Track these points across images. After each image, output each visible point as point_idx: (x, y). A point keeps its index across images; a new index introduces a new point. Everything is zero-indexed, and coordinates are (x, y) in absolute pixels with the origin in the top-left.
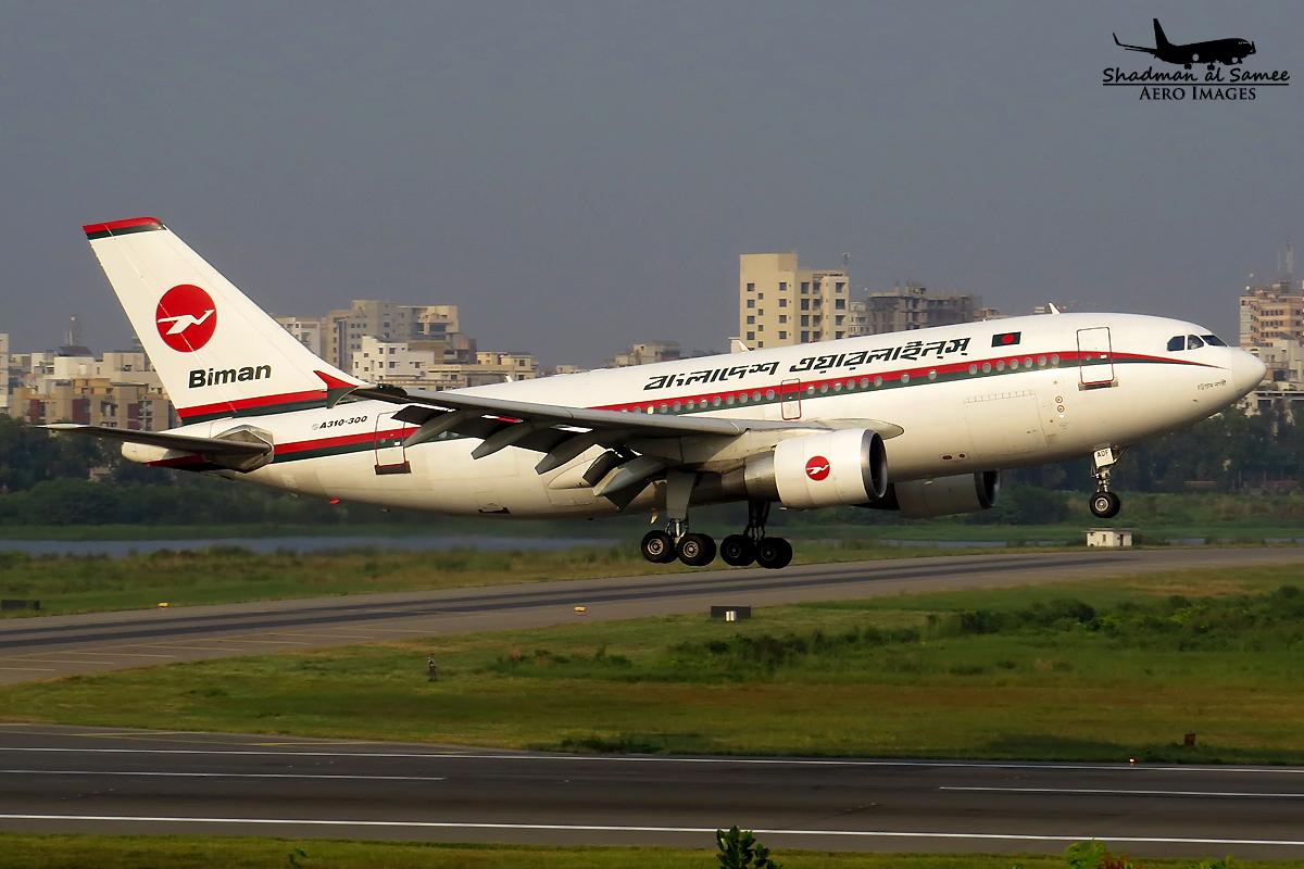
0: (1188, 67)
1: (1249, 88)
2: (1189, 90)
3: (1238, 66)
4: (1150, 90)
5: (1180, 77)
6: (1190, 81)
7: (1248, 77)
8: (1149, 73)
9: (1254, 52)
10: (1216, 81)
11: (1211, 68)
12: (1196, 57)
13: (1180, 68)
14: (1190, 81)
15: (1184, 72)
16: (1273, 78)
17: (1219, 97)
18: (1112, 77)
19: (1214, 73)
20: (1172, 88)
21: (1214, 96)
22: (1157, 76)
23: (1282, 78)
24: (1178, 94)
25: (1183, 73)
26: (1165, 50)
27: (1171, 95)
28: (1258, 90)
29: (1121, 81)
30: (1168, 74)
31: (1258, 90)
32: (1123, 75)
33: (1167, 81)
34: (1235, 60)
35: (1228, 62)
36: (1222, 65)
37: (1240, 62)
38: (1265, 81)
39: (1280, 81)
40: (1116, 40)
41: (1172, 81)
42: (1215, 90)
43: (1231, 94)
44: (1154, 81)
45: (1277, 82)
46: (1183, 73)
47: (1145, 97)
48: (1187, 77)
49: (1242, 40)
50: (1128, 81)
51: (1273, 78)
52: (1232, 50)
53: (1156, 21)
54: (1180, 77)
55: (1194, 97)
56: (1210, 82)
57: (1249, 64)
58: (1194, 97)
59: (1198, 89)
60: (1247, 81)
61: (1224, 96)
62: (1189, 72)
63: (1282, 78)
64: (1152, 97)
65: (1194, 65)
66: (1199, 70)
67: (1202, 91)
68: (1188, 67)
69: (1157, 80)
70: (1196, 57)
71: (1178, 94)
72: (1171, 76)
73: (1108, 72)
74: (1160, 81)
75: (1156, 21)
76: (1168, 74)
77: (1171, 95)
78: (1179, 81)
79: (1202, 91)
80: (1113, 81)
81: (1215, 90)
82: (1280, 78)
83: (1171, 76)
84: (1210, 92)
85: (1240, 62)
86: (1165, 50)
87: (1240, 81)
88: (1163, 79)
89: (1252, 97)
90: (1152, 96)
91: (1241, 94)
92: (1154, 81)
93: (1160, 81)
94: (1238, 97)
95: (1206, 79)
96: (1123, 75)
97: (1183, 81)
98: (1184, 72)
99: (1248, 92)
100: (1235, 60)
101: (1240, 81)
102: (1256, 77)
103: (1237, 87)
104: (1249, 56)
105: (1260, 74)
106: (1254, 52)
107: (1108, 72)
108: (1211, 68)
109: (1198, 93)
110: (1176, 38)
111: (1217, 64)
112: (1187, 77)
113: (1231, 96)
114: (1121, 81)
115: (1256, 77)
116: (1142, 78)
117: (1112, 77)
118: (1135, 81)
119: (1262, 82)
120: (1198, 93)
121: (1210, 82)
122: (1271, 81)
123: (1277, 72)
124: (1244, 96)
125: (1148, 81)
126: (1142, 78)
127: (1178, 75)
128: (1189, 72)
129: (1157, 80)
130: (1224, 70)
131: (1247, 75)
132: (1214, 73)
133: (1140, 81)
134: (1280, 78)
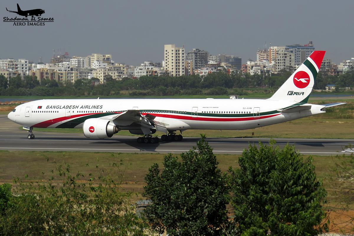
0: (26, 17)
1: (43, 22)
2: (27, 23)
3: (40, 16)
4: (16, 23)
5: (24, 19)
6: (27, 21)
7: (43, 19)
8: (16, 18)
9: (44, 13)
10: (34, 21)
11: (33, 17)
12: (28, 14)
13: (24, 17)
14: (27, 21)
15: (25, 18)
16: (49, 20)
17: (35, 25)
18: (6, 20)
19: (34, 18)
20: (22, 22)
21: (33, 24)
22: (18, 19)
23: (52, 20)
24: (24, 24)
25: (25, 18)
26: (20, 12)
27: (22, 24)
28: (45, 23)
29: (8, 20)
30: (21, 19)
31: (45, 23)
32: (9, 19)
33: (21, 20)
34: (39, 15)
35: (37, 15)
36: (35, 16)
37: (40, 15)
38: (47, 20)
39: (51, 21)
40: (7, 10)
41: (22, 21)
42: (34, 23)
43: (38, 24)
44: (17, 21)
45: (51, 21)
46: (25, 18)
47: (15, 25)
48: (26, 19)
49: (41, 9)
50: (10, 21)
51: (49, 20)
52: (38, 12)
53: (18, 4)
54: (24, 19)
55: (28, 25)
56: (32, 21)
57: (43, 16)
58: (28, 25)
59: (29, 23)
60: (42, 21)
61: (36, 24)
62: (27, 18)
63: (52, 20)
64: (16, 24)
65: (28, 16)
66: (29, 18)
67: (30, 23)
68: (26, 17)
69: (18, 20)
70: (28, 14)
71: (24, 24)
72: (22, 19)
73: (5, 18)
74: (19, 21)
75: (18, 4)
76: (21, 19)
77: (22, 24)
78: (24, 21)
79: (30, 23)
80: (6, 21)
81: (34, 23)
82: (51, 20)
83: (22, 19)
84: (32, 23)
85: (40, 15)
86: (20, 12)
87: (41, 21)
88: (20, 20)
89: (44, 25)
90: (16, 24)
91: (41, 24)
92: (17, 21)
93: (19, 21)
94: (40, 25)
95: (31, 20)
96: (9, 19)
97: (25, 21)
98: (25, 18)
99: (43, 24)
100: (39, 15)
101: (41, 21)
102: (45, 20)
103: (40, 22)
104: (43, 14)
105: (46, 19)
106: (44, 13)
107: (5, 18)
108: (33, 17)
109: (29, 24)
110: (23, 9)
111: (34, 16)
112: (26, 19)
113: (38, 25)
114: (8, 20)
115: (45, 20)
116: (14, 20)
117: (6, 20)
118: (12, 21)
119: (46, 21)
120: (29, 24)
121: (32, 21)
122: (49, 21)
123: (50, 18)
124: (41, 25)
125: (16, 20)
126: (14, 20)
127: (24, 19)
128: (27, 18)
129: (18, 20)
130: (36, 18)
131: (42, 19)
132: (34, 18)
133: (13, 21)
134: (51, 20)
